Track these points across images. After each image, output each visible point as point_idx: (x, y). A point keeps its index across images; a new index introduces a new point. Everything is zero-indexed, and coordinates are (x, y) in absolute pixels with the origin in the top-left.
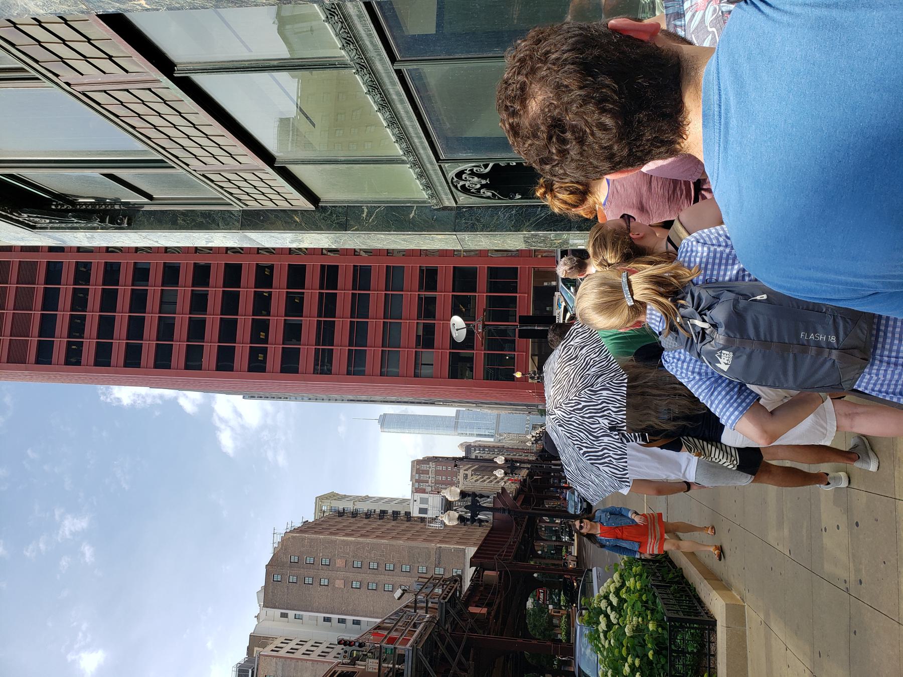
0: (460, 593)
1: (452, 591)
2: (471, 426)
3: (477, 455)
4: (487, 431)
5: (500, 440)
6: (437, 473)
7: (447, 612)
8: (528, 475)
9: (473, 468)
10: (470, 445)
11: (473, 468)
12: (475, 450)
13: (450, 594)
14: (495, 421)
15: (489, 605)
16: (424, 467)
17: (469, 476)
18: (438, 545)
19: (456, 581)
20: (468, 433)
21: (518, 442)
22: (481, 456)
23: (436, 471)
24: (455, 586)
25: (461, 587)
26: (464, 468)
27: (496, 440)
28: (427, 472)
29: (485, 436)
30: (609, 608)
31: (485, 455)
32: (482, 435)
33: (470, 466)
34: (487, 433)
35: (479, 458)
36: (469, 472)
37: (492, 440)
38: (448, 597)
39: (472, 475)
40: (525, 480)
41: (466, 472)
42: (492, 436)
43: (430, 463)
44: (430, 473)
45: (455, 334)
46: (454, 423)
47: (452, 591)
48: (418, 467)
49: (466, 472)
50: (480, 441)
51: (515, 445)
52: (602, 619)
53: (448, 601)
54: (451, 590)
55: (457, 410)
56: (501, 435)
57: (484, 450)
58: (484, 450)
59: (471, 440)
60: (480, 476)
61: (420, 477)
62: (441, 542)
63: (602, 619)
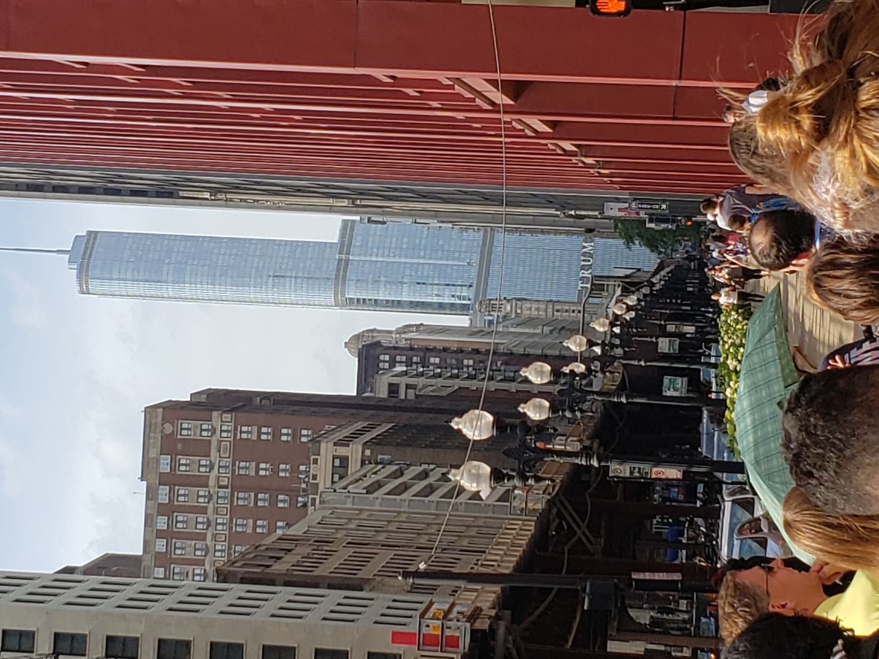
3: (395, 380)
4: (448, 291)
9: (368, 437)
10: (378, 344)
11: (368, 437)
12: (393, 363)
14: (476, 258)
16: (189, 429)
17: (354, 466)
21: (547, 329)
22: (408, 386)
26: (339, 436)
29: (441, 307)
31: (421, 381)
33: (359, 425)
34: (447, 300)
36: (354, 452)
37: (462, 321)
39: (363, 463)
41: (342, 451)
42: (464, 309)
43: (215, 414)
44: (213, 451)
48: (169, 428)
49: (342, 451)
51: (533, 345)
57: (424, 363)
58: (424, 363)
60: (395, 468)
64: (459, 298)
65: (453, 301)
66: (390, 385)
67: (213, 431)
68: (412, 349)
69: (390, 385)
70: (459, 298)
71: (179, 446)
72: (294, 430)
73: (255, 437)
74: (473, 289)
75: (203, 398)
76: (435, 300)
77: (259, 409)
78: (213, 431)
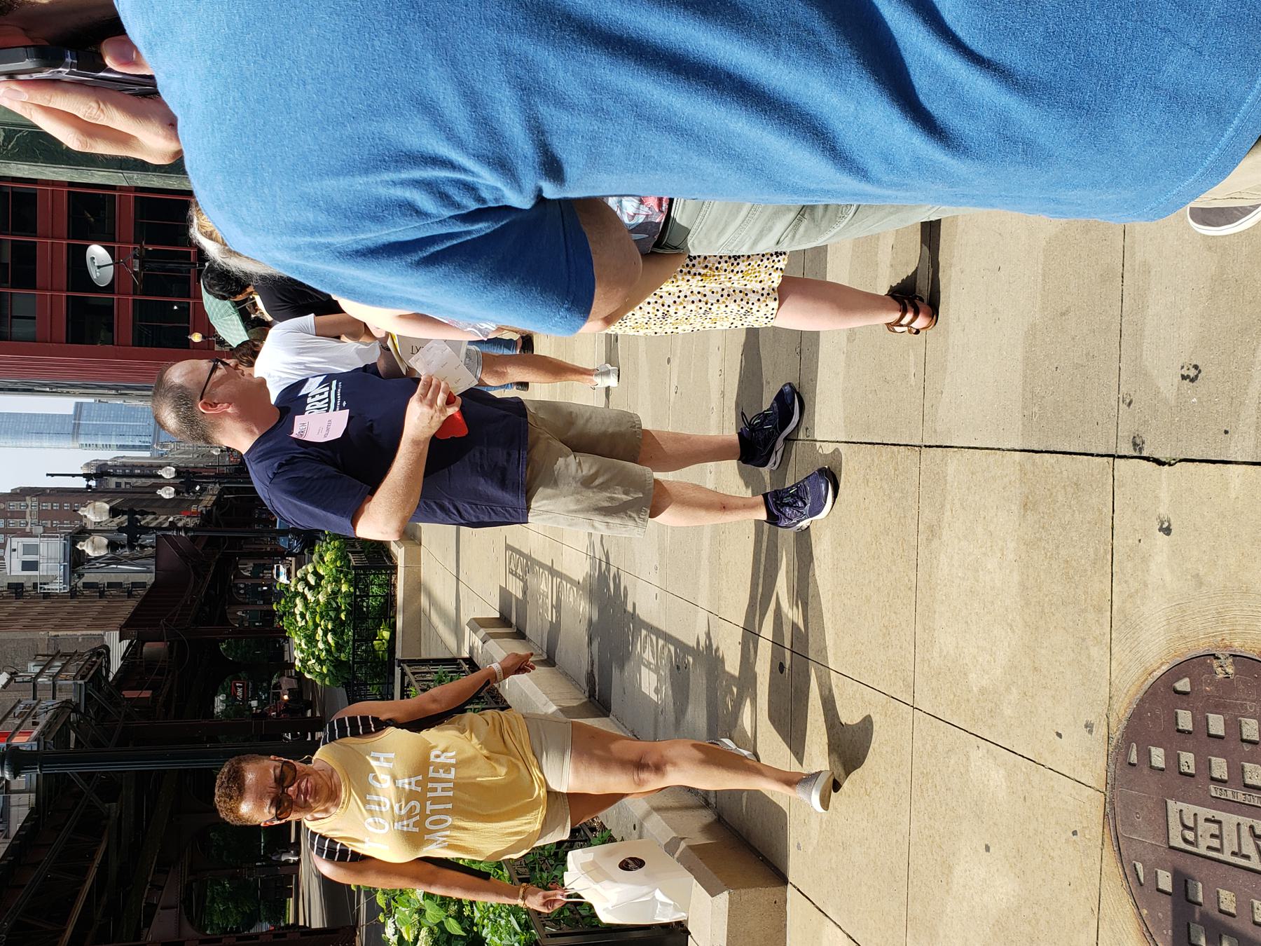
0: (108, 671)
1: (95, 668)
2: (104, 431)
4: (137, 439)
5: (162, 455)
6: (42, 515)
7: (88, 697)
8: (214, 504)
10: (106, 464)
13: (92, 672)
15: (154, 687)
18: (53, 633)
19: (99, 655)
20: (100, 443)
22: (126, 483)
23: (40, 511)
24: (99, 661)
25: (108, 662)
27: (156, 455)
28: (21, 515)
29: (134, 447)
30: (306, 589)
32: (127, 446)
34: (137, 443)
35: (123, 486)
37: (147, 454)
38: (89, 676)
40: (209, 512)
42: (147, 448)
43: (28, 498)
45: (95, 274)
46: (71, 427)
47: (95, 668)
50: (122, 457)
52: (298, 601)
53: (89, 681)
54: (93, 666)
55: (77, 403)
56: (163, 446)
59: (107, 456)
61: (6, 524)
62: (57, 627)
63: (298, 601)
64: (144, 442)
65: (140, 444)
66: (116, 483)
67: (27, 506)
68: (125, 466)
69: (116, 483)
70: (144, 442)
71: (9, 515)
72: (71, 504)
73: (50, 508)
74: (151, 437)
75: (18, 491)
76: (131, 444)
77: (49, 495)
78: (27, 506)
